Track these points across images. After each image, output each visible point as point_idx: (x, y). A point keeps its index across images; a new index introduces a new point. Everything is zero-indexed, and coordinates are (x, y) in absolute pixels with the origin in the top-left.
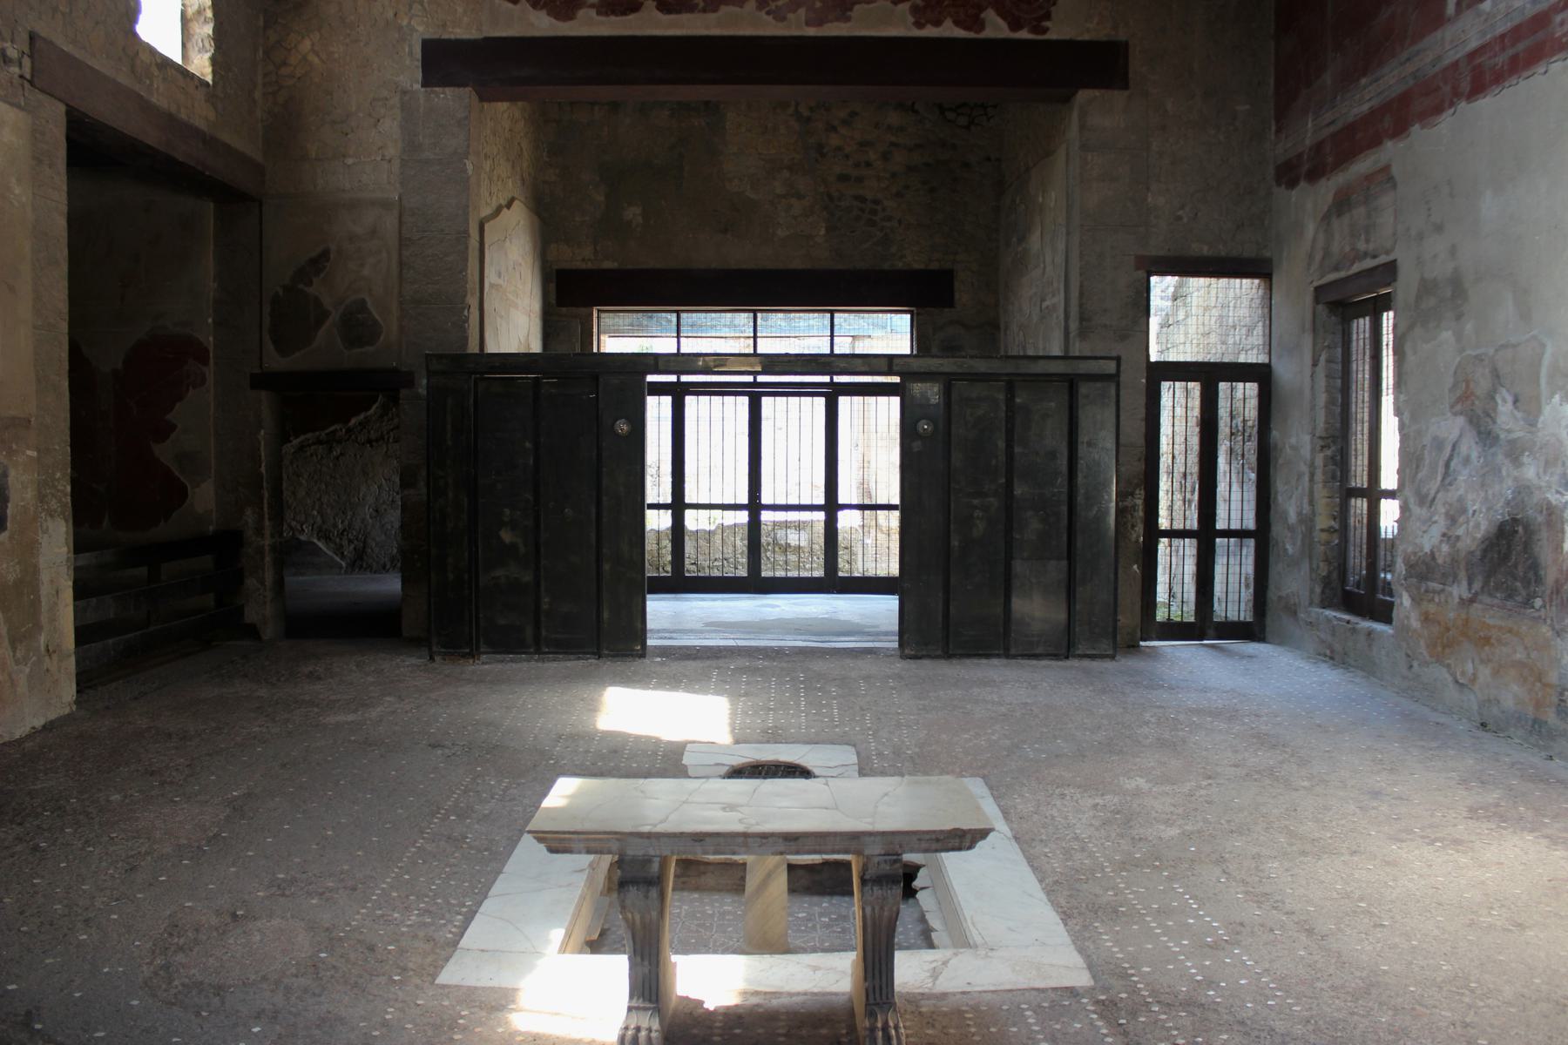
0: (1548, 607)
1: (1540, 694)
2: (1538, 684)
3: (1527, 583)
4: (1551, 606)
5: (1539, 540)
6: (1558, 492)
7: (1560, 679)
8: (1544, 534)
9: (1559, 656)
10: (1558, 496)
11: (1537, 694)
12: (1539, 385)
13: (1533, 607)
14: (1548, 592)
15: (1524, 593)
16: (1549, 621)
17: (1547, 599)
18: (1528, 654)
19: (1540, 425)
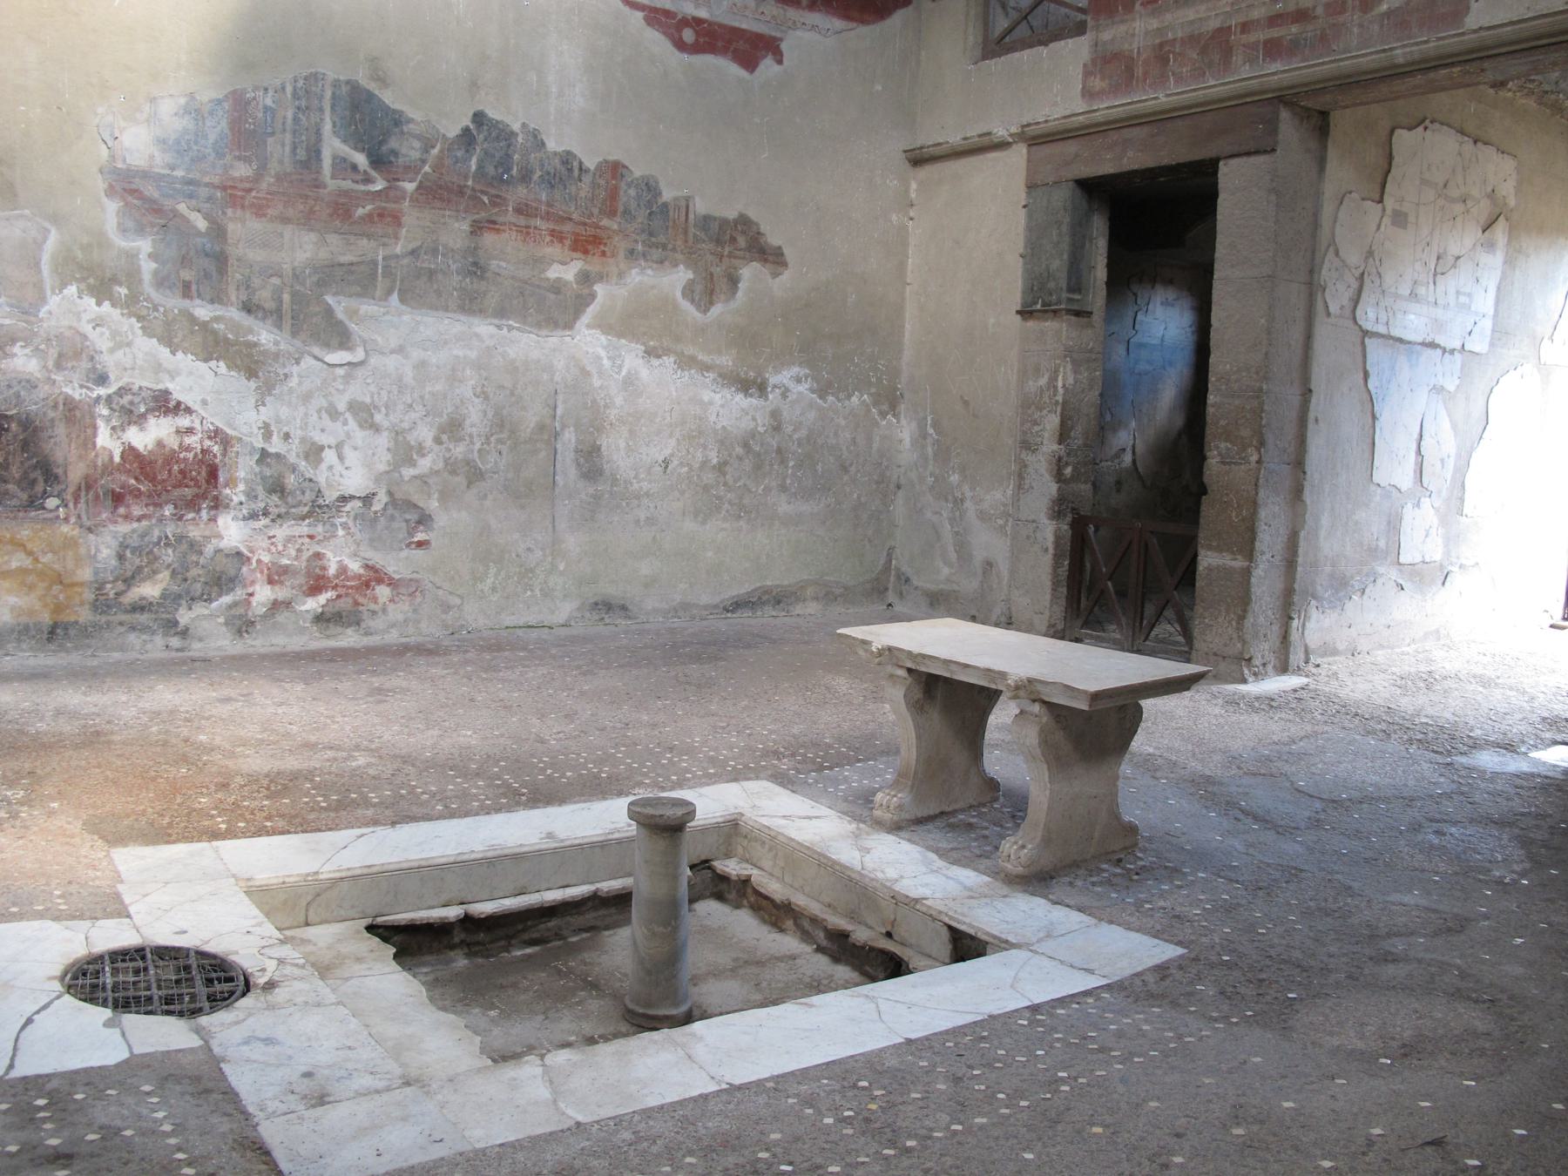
0: (71, 505)
1: (61, 597)
2: (56, 588)
3: (27, 483)
4: (76, 503)
5: (50, 437)
6: (82, 386)
7: (96, 573)
8: (61, 430)
9: (93, 552)
10: (84, 390)
11: (56, 597)
12: (40, 272)
13: (44, 508)
14: (71, 490)
15: (25, 496)
16: (73, 520)
17: (69, 497)
18: (36, 560)
19: (41, 315)
